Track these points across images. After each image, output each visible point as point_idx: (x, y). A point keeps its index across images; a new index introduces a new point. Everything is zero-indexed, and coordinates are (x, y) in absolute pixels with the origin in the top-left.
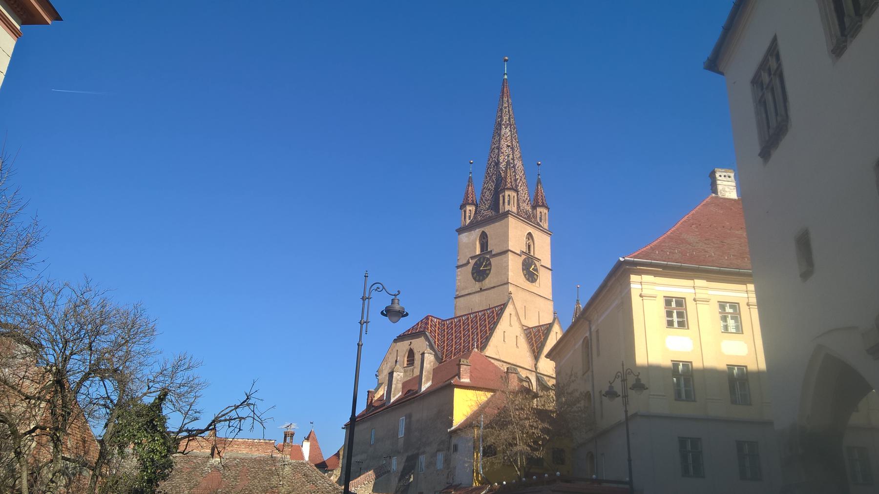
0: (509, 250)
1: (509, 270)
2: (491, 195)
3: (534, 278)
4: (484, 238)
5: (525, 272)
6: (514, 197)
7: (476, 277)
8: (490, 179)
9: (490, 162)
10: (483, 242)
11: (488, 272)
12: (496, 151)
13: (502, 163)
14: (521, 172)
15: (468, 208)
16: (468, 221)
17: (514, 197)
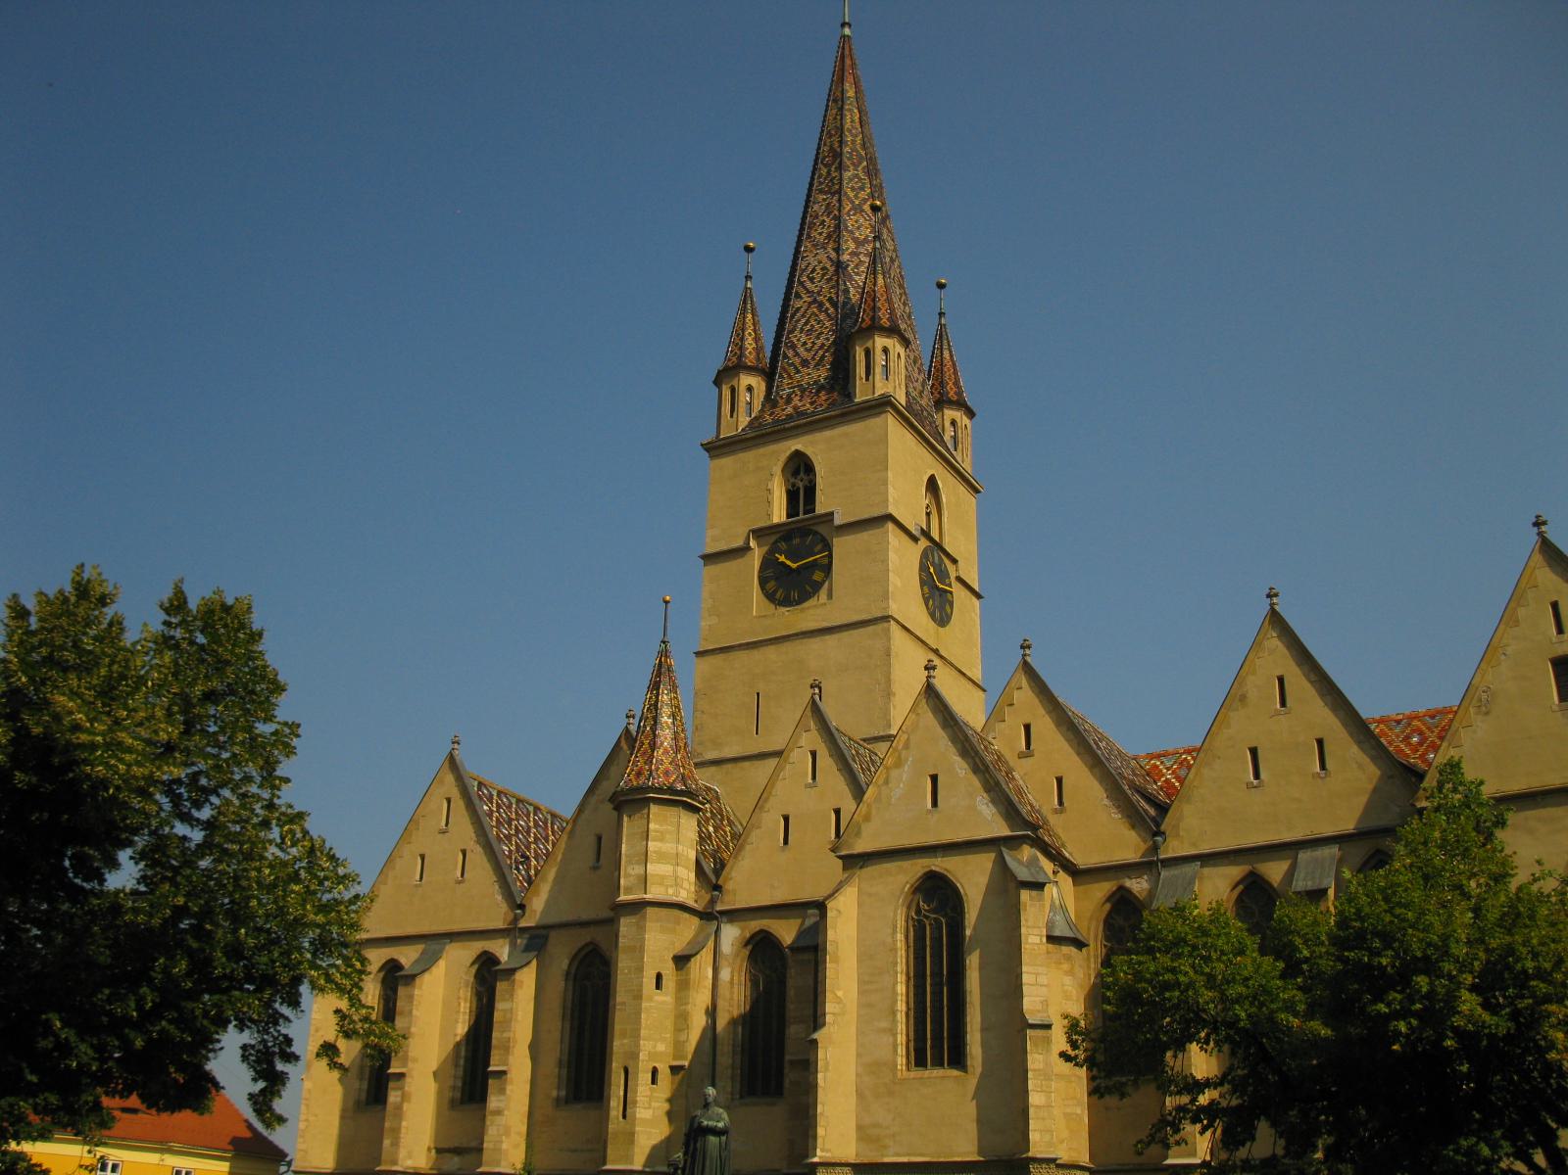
0: (890, 518)
3: (947, 614)
5: (926, 589)
7: (775, 592)
11: (818, 576)
15: (746, 380)
16: (744, 420)
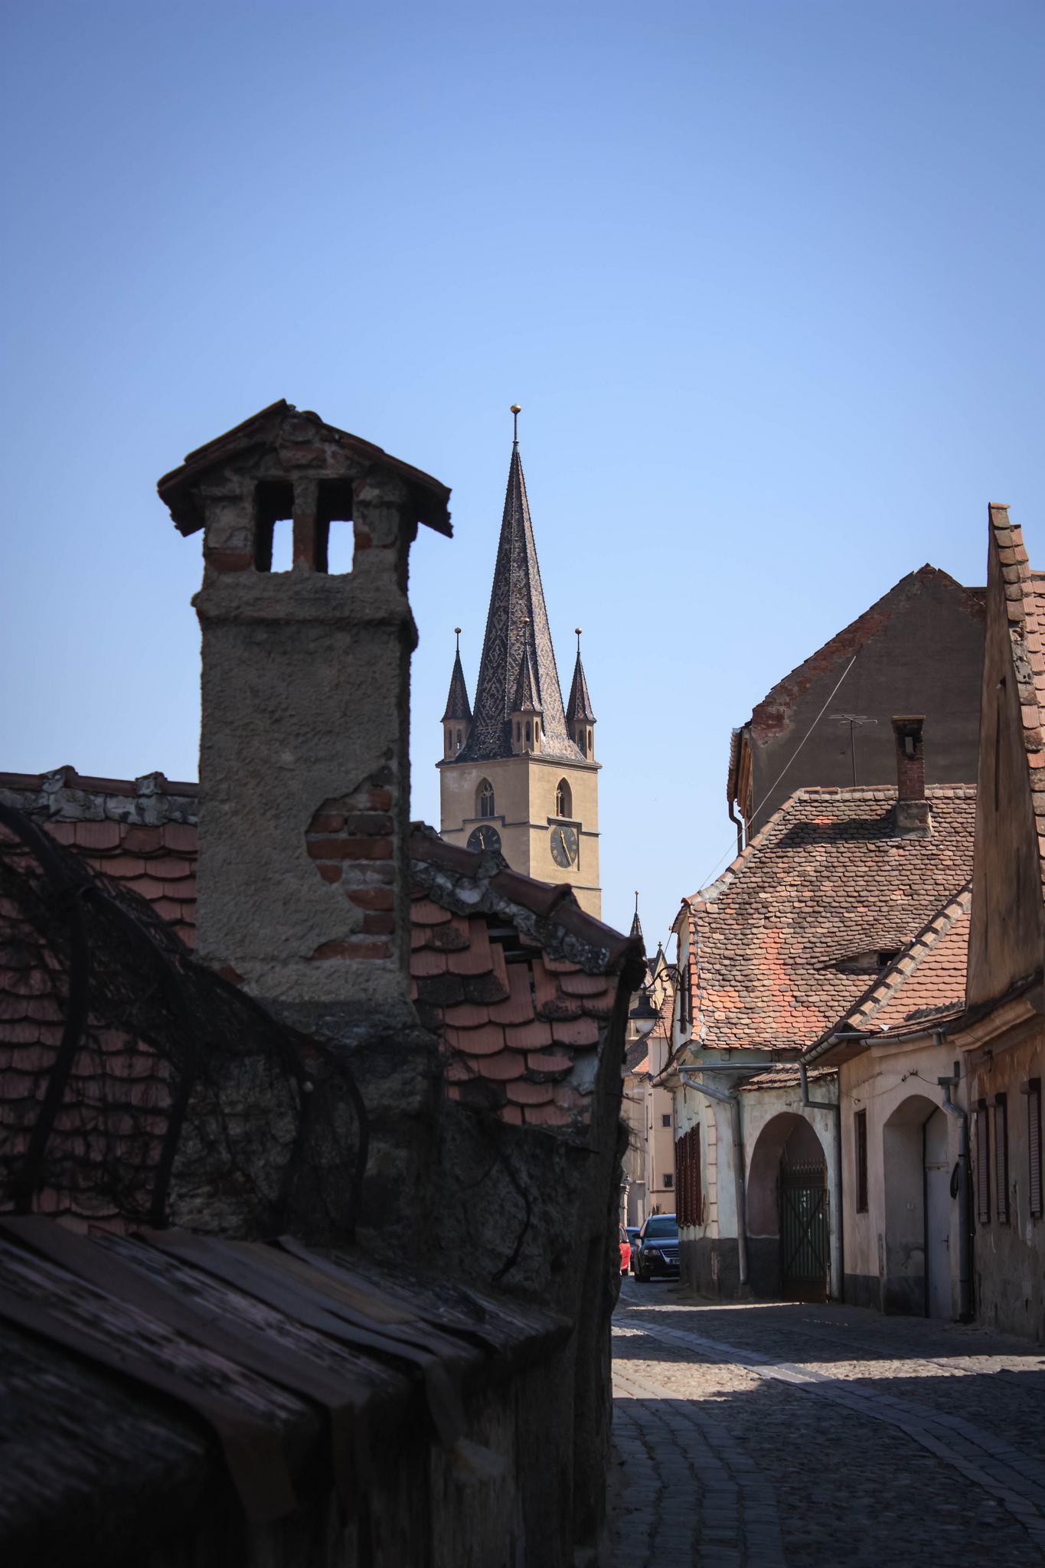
1: (531, 859)
2: (497, 708)
4: (486, 790)
5: (555, 852)
6: (537, 723)
8: (493, 674)
9: (492, 636)
10: (484, 795)
12: (504, 617)
13: (513, 644)
14: (548, 656)
17: (537, 723)
